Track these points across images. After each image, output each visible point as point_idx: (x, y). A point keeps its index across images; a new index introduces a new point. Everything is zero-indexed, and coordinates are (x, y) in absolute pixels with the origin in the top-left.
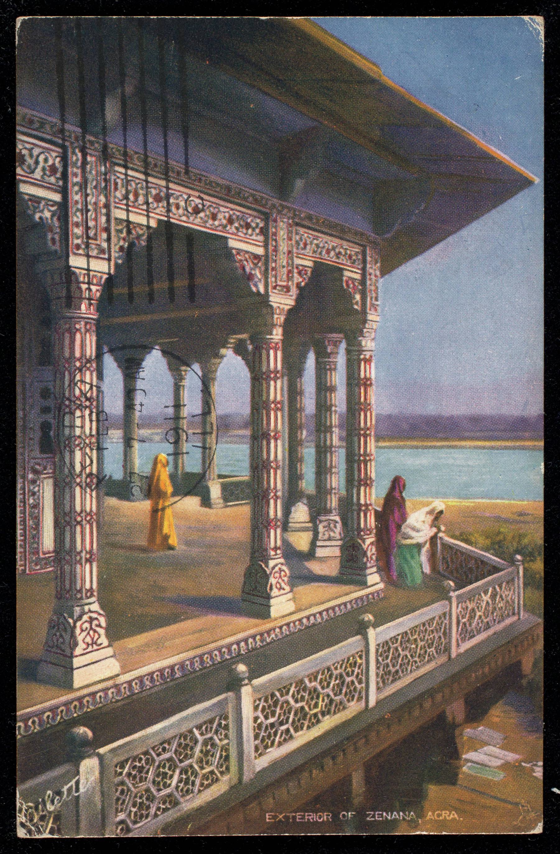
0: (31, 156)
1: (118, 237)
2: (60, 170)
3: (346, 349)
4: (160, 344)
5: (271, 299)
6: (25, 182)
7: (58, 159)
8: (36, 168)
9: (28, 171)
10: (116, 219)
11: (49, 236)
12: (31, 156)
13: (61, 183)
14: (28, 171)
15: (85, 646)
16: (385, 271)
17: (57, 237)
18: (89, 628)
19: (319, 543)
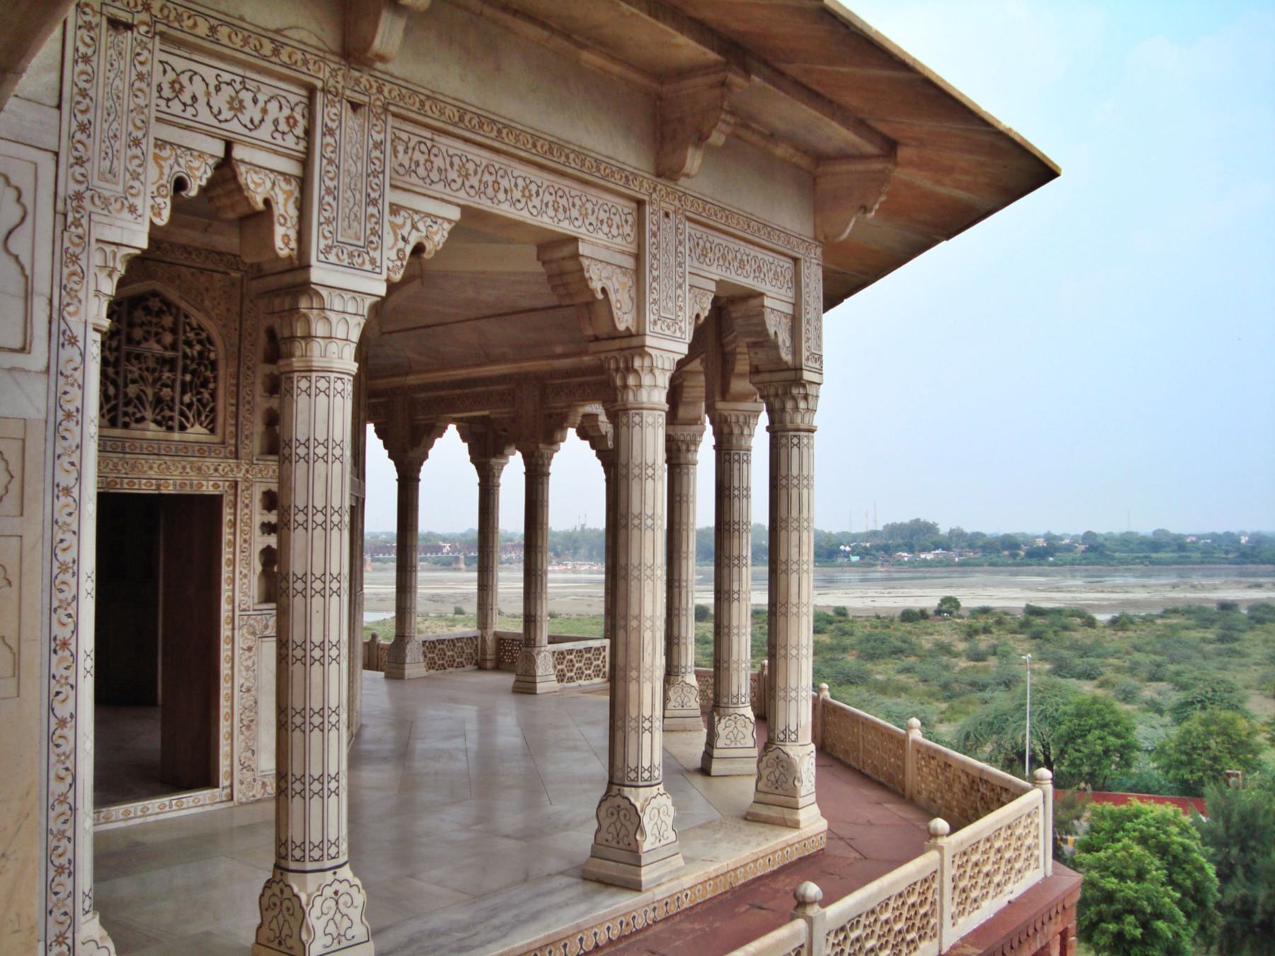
0: (255, 101)
1: (395, 234)
2: (302, 123)
3: (768, 429)
4: (454, 421)
5: (649, 341)
6: (243, 143)
7: (299, 110)
8: (262, 120)
9: (250, 126)
10: (391, 205)
11: (279, 231)
12: (255, 101)
13: (302, 146)
14: (250, 126)
15: (328, 940)
16: (831, 300)
17: (293, 234)
18: (332, 912)
19: (716, 753)
